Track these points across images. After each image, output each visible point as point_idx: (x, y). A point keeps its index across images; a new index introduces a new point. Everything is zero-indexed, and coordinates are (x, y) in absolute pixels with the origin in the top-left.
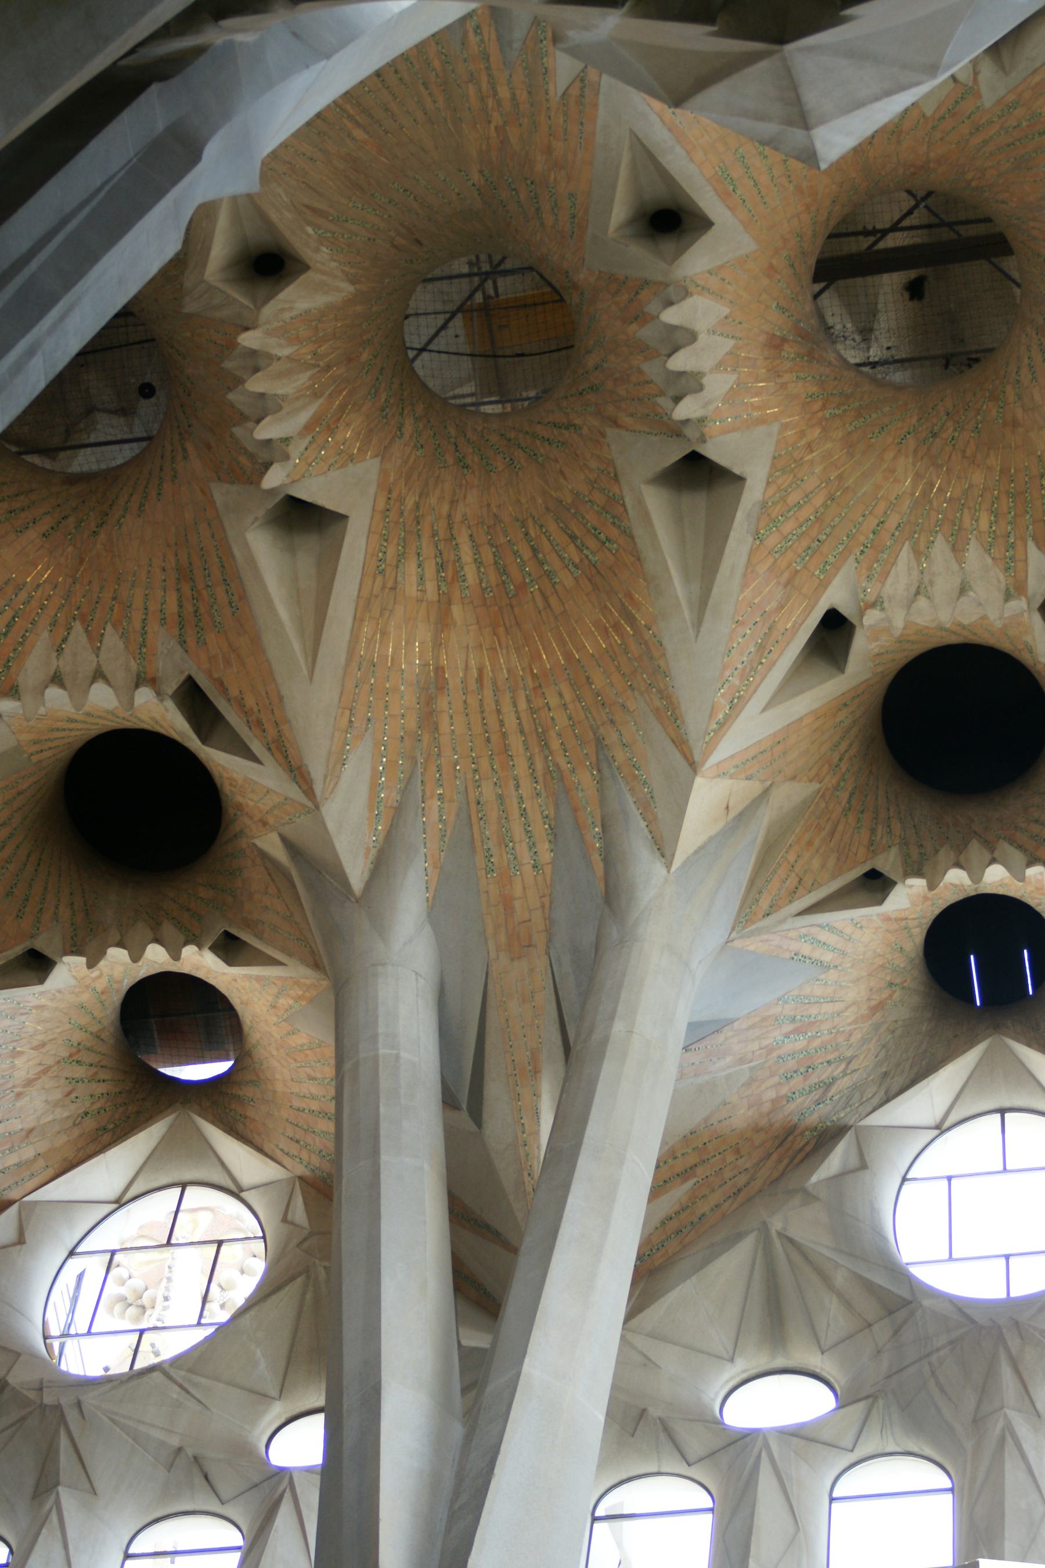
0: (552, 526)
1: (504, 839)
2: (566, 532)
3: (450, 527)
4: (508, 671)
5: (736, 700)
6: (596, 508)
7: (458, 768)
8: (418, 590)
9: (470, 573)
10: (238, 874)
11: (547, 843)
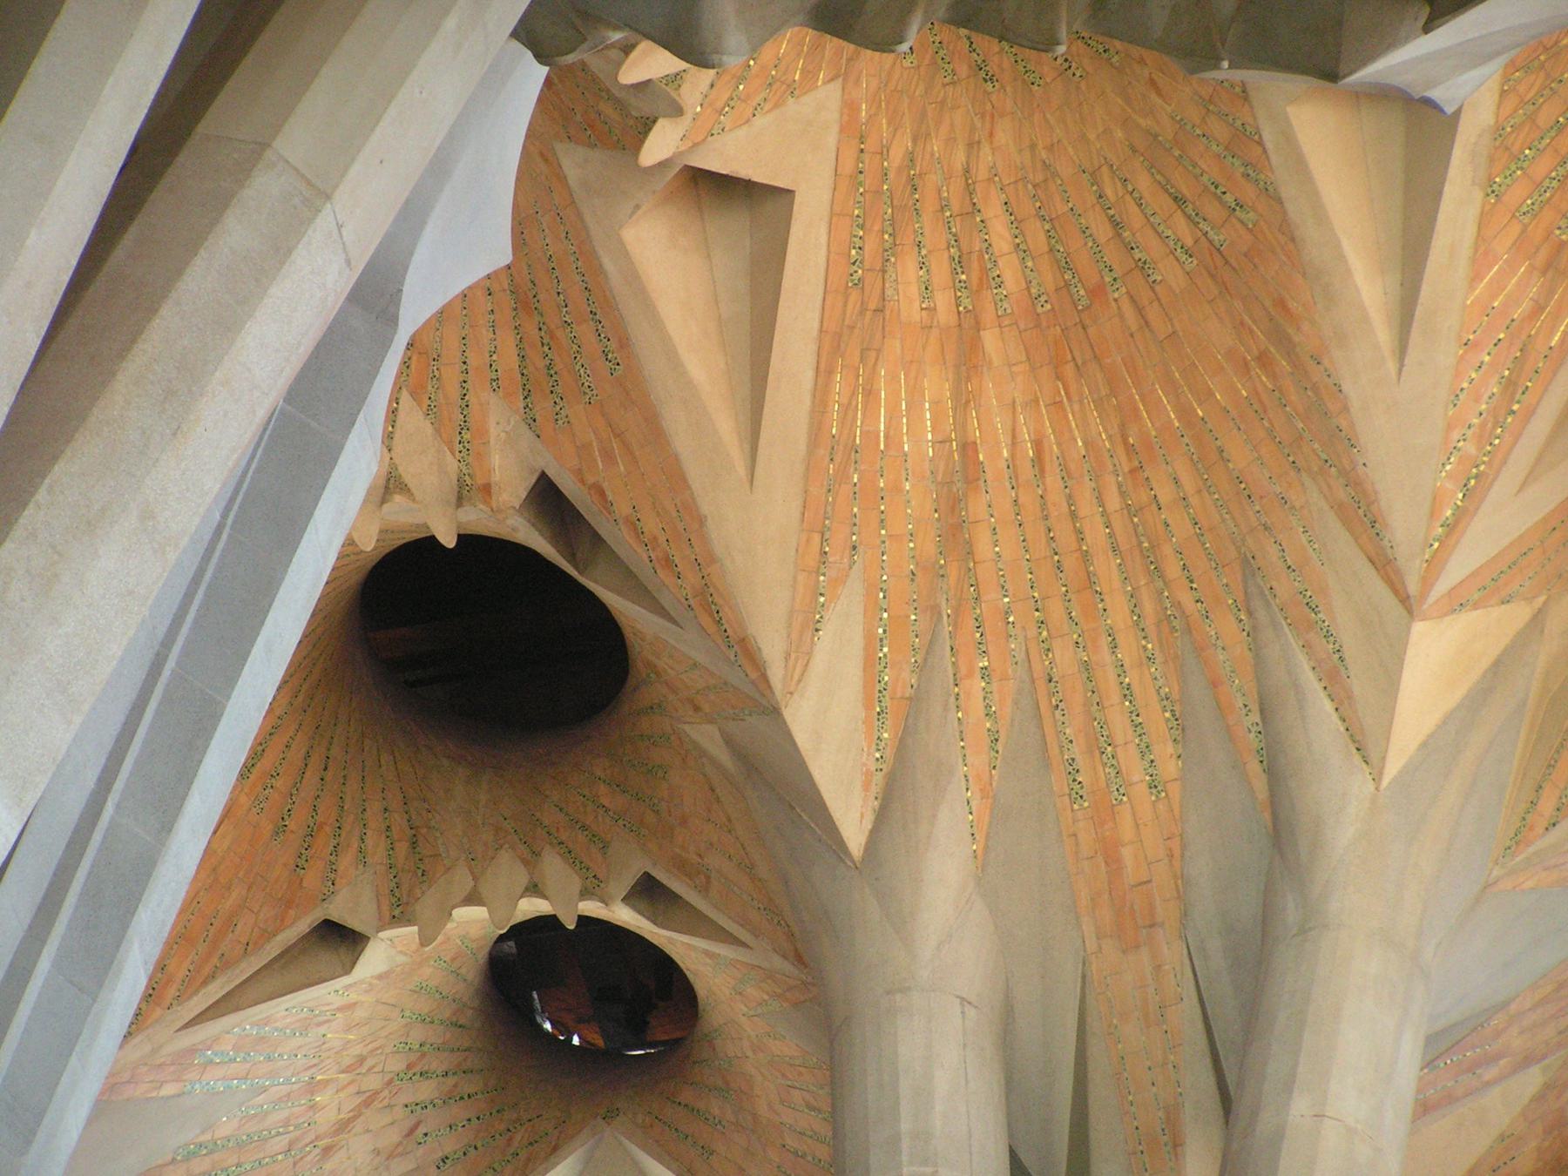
0: (1143, 182)
1: (1097, 739)
2: (1167, 191)
3: (969, 190)
4: (1085, 443)
5: (1473, 482)
6: (1214, 147)
7: (1011, 619)
8: (922, 309)
9: (1009, 271)
10: (660, 774)
11: (1170, 743)
